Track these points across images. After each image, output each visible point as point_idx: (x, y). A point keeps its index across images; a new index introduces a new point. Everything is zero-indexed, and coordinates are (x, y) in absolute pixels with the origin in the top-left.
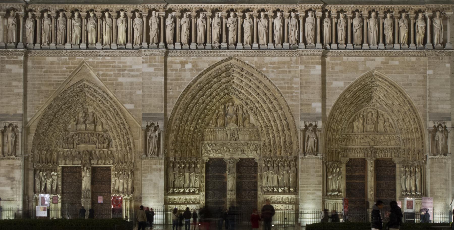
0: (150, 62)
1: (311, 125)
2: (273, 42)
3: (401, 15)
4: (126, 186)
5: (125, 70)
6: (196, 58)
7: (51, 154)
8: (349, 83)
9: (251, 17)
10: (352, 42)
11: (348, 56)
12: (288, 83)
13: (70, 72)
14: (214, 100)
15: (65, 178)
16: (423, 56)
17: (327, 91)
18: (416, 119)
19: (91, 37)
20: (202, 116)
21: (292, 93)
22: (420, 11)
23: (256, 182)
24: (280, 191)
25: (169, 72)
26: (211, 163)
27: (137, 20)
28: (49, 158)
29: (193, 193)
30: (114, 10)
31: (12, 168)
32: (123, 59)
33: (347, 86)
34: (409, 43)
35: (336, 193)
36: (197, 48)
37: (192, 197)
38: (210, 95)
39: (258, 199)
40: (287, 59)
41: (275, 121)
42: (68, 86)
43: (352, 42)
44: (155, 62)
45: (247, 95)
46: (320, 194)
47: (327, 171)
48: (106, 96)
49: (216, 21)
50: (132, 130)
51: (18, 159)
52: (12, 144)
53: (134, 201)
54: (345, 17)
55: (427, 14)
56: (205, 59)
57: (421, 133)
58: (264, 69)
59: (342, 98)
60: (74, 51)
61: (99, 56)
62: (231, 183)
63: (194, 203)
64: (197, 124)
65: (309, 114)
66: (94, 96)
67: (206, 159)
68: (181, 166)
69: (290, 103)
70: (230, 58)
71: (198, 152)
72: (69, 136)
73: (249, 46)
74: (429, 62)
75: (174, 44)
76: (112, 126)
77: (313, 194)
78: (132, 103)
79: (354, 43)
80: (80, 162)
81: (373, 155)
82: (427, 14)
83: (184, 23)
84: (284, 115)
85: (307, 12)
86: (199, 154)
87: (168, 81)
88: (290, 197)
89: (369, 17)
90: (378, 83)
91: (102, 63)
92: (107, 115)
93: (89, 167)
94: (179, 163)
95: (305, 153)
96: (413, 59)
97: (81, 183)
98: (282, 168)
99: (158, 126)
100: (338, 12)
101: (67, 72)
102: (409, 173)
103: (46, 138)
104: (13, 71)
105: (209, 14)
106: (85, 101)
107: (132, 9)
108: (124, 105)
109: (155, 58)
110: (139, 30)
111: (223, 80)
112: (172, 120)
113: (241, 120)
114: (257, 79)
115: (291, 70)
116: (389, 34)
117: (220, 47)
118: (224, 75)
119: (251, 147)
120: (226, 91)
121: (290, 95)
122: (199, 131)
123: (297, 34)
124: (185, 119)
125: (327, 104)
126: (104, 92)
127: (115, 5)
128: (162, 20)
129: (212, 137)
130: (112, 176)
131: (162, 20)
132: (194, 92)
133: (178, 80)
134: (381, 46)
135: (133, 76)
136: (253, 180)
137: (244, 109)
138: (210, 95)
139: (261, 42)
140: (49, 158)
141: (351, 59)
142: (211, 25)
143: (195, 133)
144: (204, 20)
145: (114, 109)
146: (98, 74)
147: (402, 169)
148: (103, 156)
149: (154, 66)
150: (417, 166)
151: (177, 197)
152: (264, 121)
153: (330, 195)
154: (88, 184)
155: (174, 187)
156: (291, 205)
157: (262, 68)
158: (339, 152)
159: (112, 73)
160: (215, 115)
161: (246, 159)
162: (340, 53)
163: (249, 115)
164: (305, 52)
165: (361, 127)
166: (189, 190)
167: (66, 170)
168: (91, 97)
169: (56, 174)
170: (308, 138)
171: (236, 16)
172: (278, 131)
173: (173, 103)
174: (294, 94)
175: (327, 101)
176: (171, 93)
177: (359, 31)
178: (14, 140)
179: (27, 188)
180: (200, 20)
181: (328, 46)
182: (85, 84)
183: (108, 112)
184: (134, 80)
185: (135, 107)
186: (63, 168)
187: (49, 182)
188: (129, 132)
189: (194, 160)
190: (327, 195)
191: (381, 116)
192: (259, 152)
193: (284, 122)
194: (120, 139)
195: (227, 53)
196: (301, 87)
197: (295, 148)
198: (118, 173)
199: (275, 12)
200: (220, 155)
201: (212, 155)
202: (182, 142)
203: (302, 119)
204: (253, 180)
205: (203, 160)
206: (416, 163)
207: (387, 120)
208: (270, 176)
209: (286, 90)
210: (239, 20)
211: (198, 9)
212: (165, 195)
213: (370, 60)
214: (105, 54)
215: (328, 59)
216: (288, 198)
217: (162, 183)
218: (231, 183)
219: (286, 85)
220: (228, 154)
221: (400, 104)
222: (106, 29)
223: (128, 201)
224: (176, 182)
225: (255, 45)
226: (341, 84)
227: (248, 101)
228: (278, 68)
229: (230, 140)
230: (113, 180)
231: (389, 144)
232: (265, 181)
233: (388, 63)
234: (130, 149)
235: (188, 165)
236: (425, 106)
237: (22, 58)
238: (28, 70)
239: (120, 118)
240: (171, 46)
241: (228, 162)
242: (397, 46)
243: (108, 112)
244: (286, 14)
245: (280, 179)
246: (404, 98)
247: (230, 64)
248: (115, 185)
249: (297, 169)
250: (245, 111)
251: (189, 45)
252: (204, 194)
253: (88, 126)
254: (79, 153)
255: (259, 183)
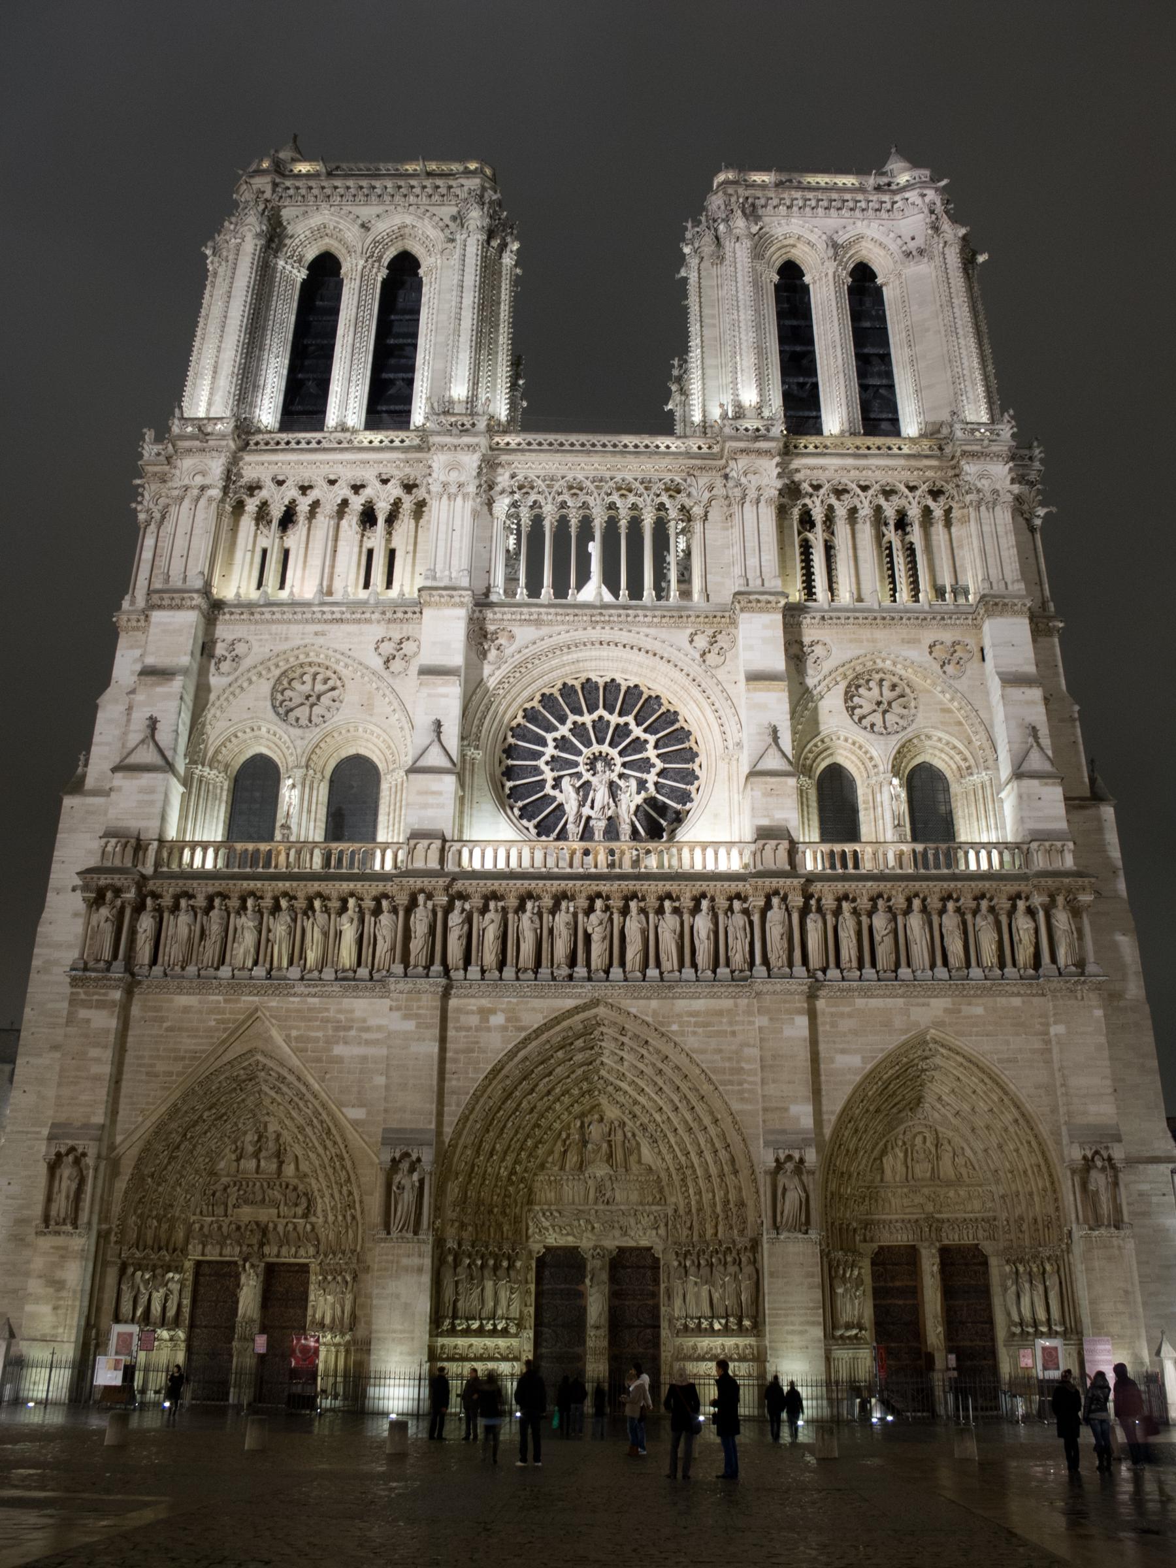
0: (407, 1008)
1: (789, 1158)
2: (694, 965)
3: (978, 905)
4: (338, 1312)
5: (350, 1028)
6: (514, 1000)
7: (172, 1228)
8: (874, 1058)
9: (643, 911)
10: (874, 964)
11: (866, 996)
12: (730, 1059)
13: (225, 1030)
14: (557, 1106)
15: (202, 1290)
16: (1037, 995)
17: (823, 1078)
18: (1034, 1143)
19: (281, 952)
20: (530, 1143)
21: (740, 1084)
22: (1018, 896)
23: (656, 1307)
24: (717, 1326)
25: (451, 1033)
26: (548, 1259)
27: (385, 919)
28: (164, 1236)
29: (505, 1333)
30: (334, 895)
31: (62, 1257)
32: (347, 1003)
33: (869, 1067)
34: (1002, 966)
35: (854, 1332)
36: (518, 979)
37: (502, 1342)
38: (549, 1093)
39: (662, 1348)
40: (727, 1003)
41: (700, 1153)
42: (218, 1064)
43: (874, 964)
44: (419, 1008)
45: (634, 1094)
46: (818, 1332)
47: (831, 1277)
48: (303, 1089)
49: (561, 920)
50: (359, 1172)
51: (80, 1235)
52: (67, 1197)
53: (356, 1351)
54: (855, 912)
55: (1038, 900)
56: (537, 1003)
57: (1051, 1175)
58: (675, 1027)
59: (859, 1094)
60: (235, 986)
61: (294, 995)
62: (596, 1307)
63: (505, 1359)
64: (517, 1162)
65: (783, 1132)
66: (278, 1091)
67: (537, 1248)
68: (473, 1262)
69: (736, 1106)
70: (595, 1003)
71: (517, 1232)
72: (219, 1187)
73: (639, 974)
74: (1055, 1007)
75: (466, 970)
76: (317, 1163)
77: (801, 1333)
78: (361, 1106)
79: (879, 966)
80: (237, 1249)
81: (933, 1235)
82: (1038, 900)
83: (490, 927)
84: (723, 1136)
85: (768, 899)
86: (520, 1236)
87: (449, 1055)
88: (742, 1341)
89: (908, 911)
90: (938, 1060)
91: (299, 1011)
92: (306, 1136)
93: (256, 1262)
94: (469, 1256)
95: (776, 1227)
96: (1017, 1001)
97: (237, 1302)
98: (721, 1268)
99: (419, 1160)
100: (839, 900)
101: (217, 1030)
102: (1026, 1278)
103: (160, 1189)
104: (93, 1025)
105: (548, 902)
106: (259, 1104)
107: (374, 893)
108: (344, 1110)
109: (419, 1000)
110: (388, 939)
111: (579, 1057)
112: (455, 1146)
113: (620, 1154)
114: (658, 1052)
115: (736, 1028)
116: (955, 947)
117: (571, 977)
118: (579, 1043)
119: (645, 1221)
120: (585, 1086)
121: (736, 1088)
122: (523, 1180)
123: (747, 948)
124: (486, 1147)
125: (824, 1109)
126: (299, 1079)
127: (337, 884)
128: (440, 915)
129: (551, 1196)
130: (312, 1287)
131: (440, 915)
132: (508, 1082)
133: (472, 1051)
134: (941, 972)
135: (368, 1043)
136: (650, 1302)
137: (627, 1129)
138: (549, 1093)
139: (666, 965)
140: (164, 1236)
141: (874, 1003)
142: (551, 931)
143: (513, 1183)
144: (536, 918)
145: (322, 1122)
146: (288, 1036)
147: (1007, 1268)
148: (293, 1235)
149: (418, 1016)
150: (1045, 1258)
151: (461, 1342)
152: (675, 1157)
153: (841, 1337)
154: (251, 1305)
155: (455, 1316)
156: (746, 1365)
157: (669, 1024)
158: (855, 1230)
159: (320, 1034)
160: (559, 1143)
161: (632, 1249)
162: (849, 990)
163: (638, 1144)
164: (769, 987)
165: (900, 1168)
166: (495, 1325)
167: (206, 1270)
168: (272, 1093)
169: (177, 1277)
170: (785, 1189)
171: (607, 908)
172: (709, 1177)
173: (458, 1105)
174: (746, 1086)
175: (824, 1101)
176: (454, 1083)
177: (889, 940)
178: (74, 1186)
179: (98, 1309)
180: (526, 918)
181: (819, 974)
182: (258, 1062)
183: (308, 1130)
184: (371, 1051)
185: (368, 1114)
186: (198, 1264)
187: (158, 1297)
188: (353, 1178)
189: (506, 1248)
190: (833, 1337)
191: (945, 1142)
192: (662, 1231)
193: (723, 1154)
194: (332, 1196)
195: (586, 992)
196: (762, 1067)
197: (751, 1217)
198: (325, 1278)
199: (697, 900)
200: (570, 1238)
201: (554, 1239)
202: (480, 1202)
203: (767, 1144)
204: (650, 1302)
205: (530, 1252)
206: (1045, 1252)
207: (959, 1151)
208: (691, 1289)
209: (727, 1077)
210: (616, 917)
211: (522, 891)
212: (431, 1336)
213: (918, 1005)
214: (306, 991)
215: (821, 1004)
216: (737, 1346)
217: (423, 1305)
218: (596, 1307)
219: (727, 1065)
220: (590, 1235)
221: (991, 1110)
222: (315, 936)
223: (342, 1349)
224: (460, 1304)
225: (652, 972)
226: (855, 1061)
227: (637, 1110)
228: (706, 1025)
229: (596, 1203)
230: (312, 1297)
231: (969, 1208)
232: (678, 1302)
233: (959, 1011)
234: (354, 1217)
235: (491, 1262)
236: (1054, 1110)
237: (117, 995)
238: (131, 1024)
239: (335, 1143)
240: (457, 975)
241: (588, 1256)
242: (975, 972)
243: (308, 1130)
244: (722, 903)
245: (716, 1296)
246: (1001, 1093)
247: (595, 1017)
248: (315, 1308)
249: (757, 1271)
250: (629, 1135)
251: (501, 971)
252: (532, 1335)
253: (263, 1163)
254: (238, 1228)
255: (663, 1309)
